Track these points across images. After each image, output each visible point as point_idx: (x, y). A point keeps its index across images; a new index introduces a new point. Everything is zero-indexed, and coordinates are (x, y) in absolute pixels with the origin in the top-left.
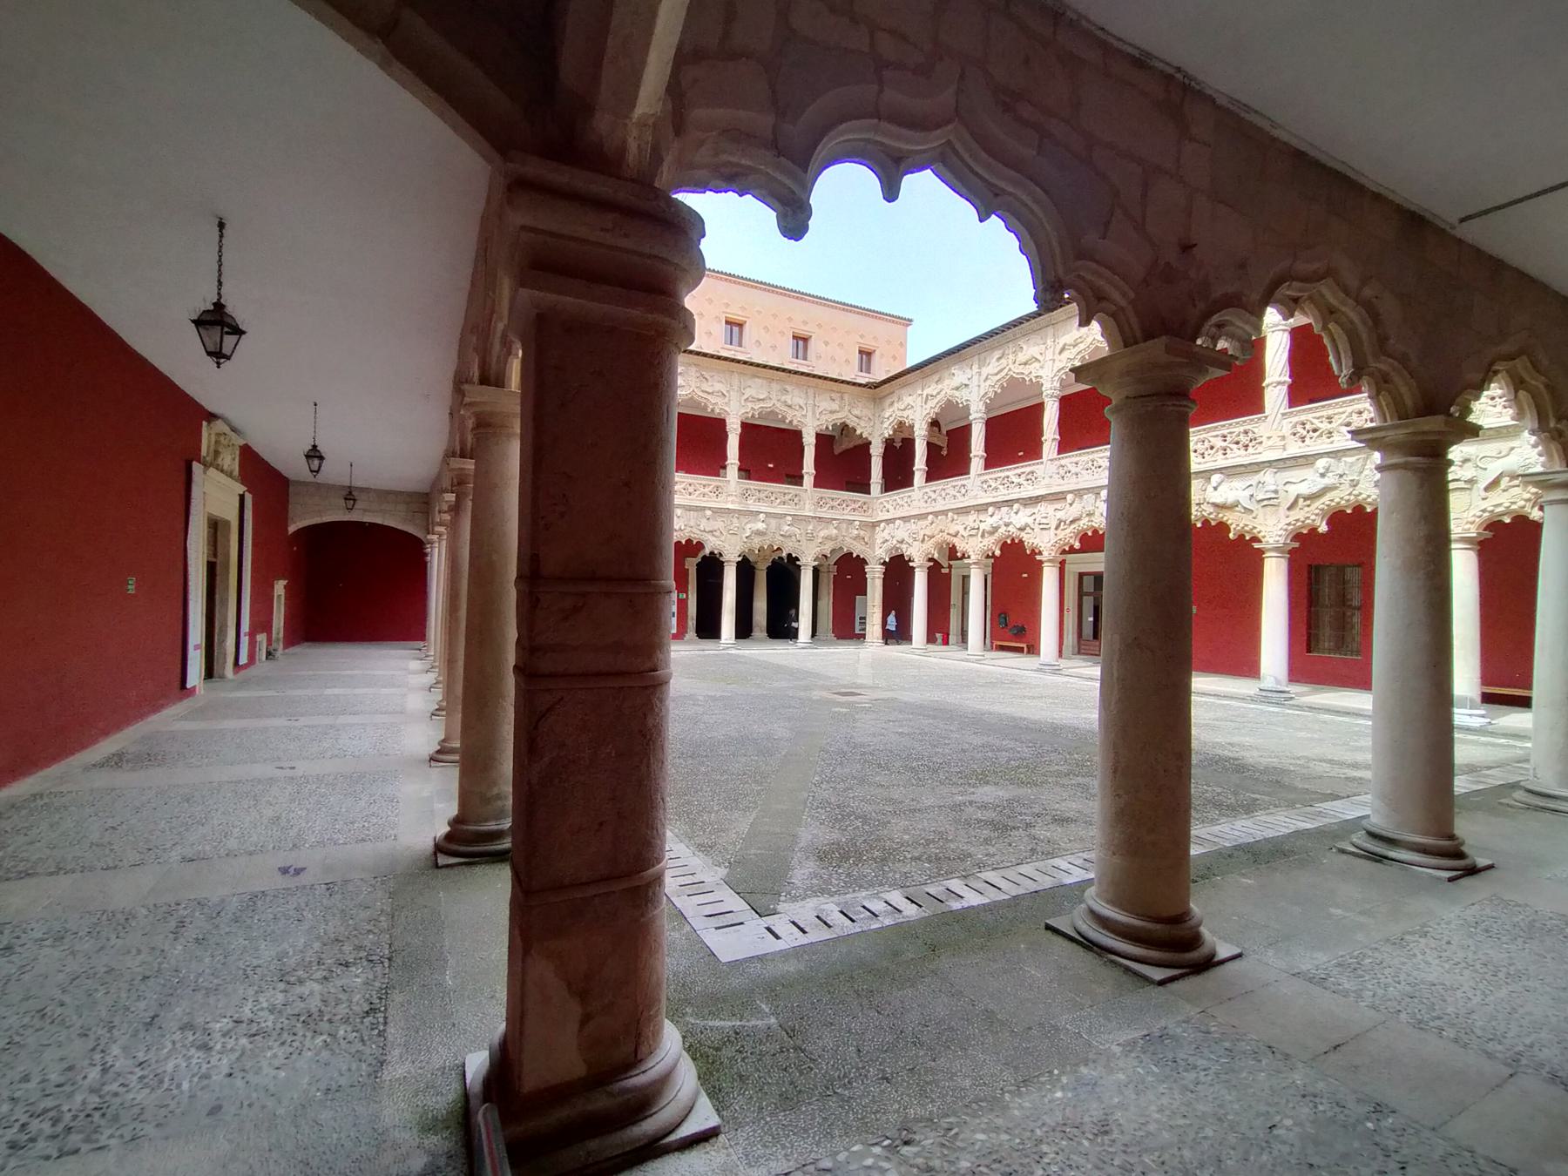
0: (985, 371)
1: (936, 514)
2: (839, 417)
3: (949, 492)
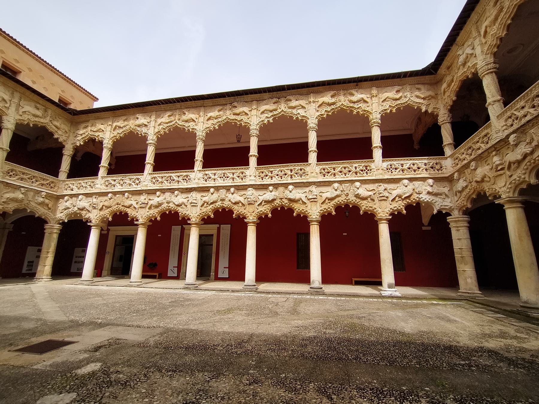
0: (160, 121)
1: (115, 193)
2: (45, 121)
3: (125, 182)
